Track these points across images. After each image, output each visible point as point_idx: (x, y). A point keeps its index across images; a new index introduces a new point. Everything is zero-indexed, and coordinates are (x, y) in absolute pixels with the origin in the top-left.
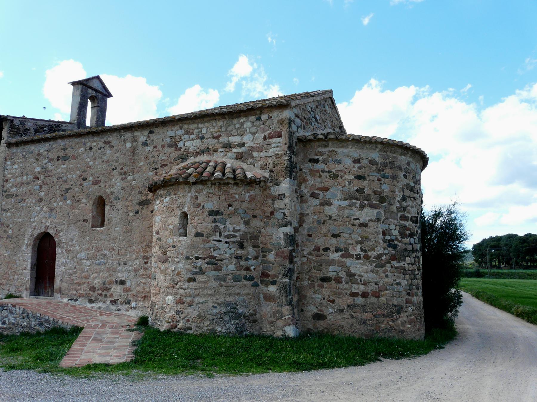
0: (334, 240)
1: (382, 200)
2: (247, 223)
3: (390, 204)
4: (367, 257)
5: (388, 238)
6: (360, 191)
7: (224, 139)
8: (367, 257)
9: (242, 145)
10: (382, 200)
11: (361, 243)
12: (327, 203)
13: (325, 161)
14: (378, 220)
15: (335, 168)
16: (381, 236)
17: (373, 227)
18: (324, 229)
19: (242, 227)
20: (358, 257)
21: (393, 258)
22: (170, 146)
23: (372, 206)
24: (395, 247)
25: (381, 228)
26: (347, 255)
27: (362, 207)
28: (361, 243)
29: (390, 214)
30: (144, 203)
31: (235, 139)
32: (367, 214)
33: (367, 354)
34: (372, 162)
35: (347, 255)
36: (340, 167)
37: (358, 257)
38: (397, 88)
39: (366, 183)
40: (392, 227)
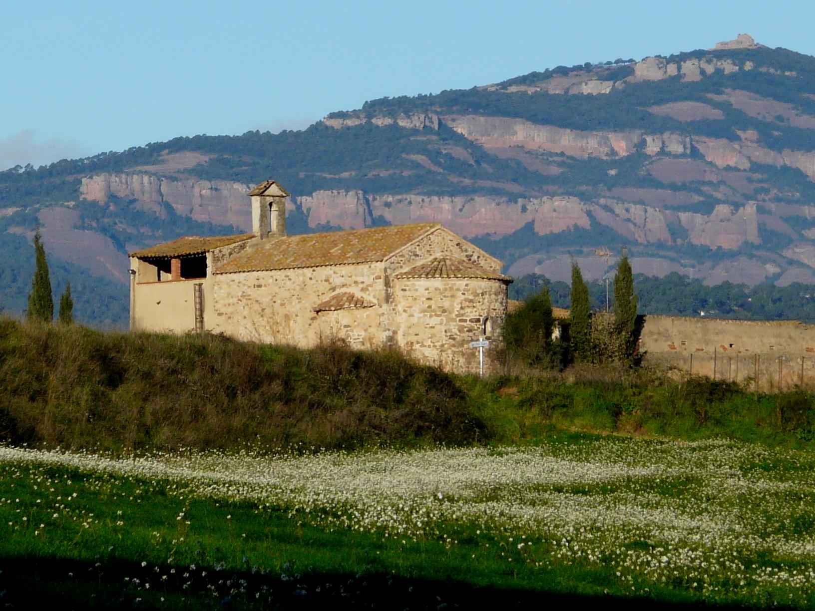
0: (416, 338)
1: (444, 311)
2: (366, 330)
3: (450, 313)
4: (435, 346)
5: (449, 334)
6: (430, 307)
7: (354, 278)
8: (435, 346)
9: (363, 282)
10: (444, 311)
11: (431, 338)
12: (411, 315)
13: (410, 290)
14: (441, 324)
15: (415, 294)
16: (444, 333)
17: (438, 328)
18: (411, 331)
19: (363, 333)
20: (429, 346)
21: (454, 346)
22: (326, 281)
23: (437, 315)
24: (454, 339)
25: (443, 328)
26: (423, 346)
27: (431, 316)
28: (431, 338)
29: (450, 320)
30: (313, 319)
31: (360, 279)
32: (434, 321)
33: (507, 543)
34: (436, 289)
35: (423, 346)
36: (418, 294)
37: (429, 346)
38: (236, 138)
39: (433, 302)
40: (452, 327)
